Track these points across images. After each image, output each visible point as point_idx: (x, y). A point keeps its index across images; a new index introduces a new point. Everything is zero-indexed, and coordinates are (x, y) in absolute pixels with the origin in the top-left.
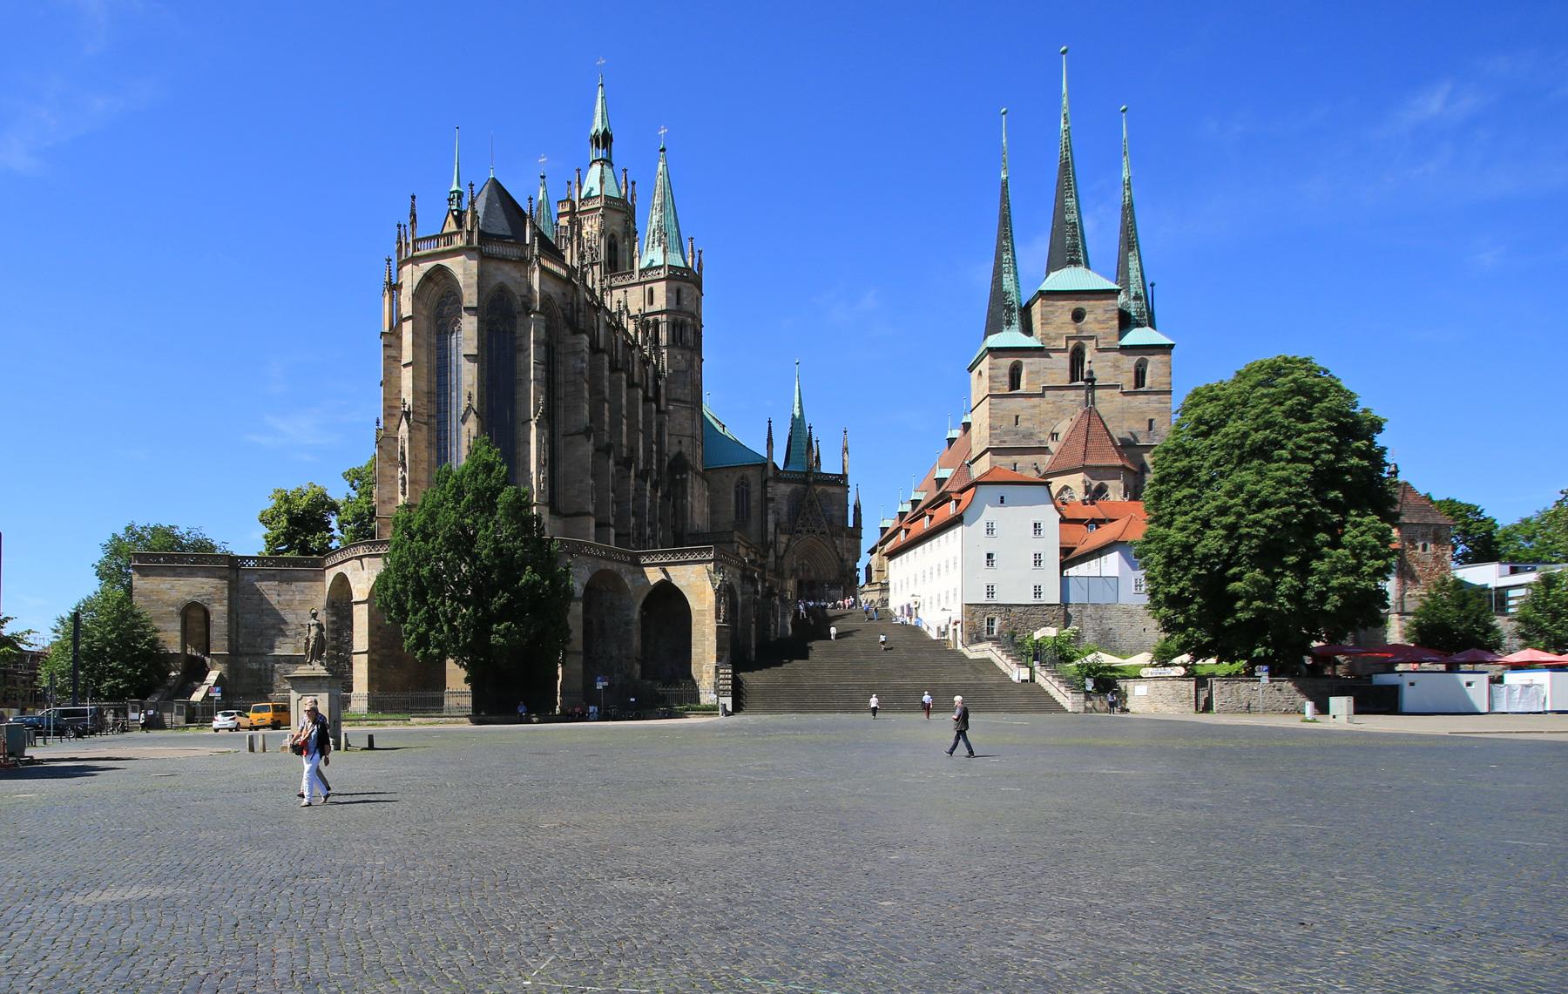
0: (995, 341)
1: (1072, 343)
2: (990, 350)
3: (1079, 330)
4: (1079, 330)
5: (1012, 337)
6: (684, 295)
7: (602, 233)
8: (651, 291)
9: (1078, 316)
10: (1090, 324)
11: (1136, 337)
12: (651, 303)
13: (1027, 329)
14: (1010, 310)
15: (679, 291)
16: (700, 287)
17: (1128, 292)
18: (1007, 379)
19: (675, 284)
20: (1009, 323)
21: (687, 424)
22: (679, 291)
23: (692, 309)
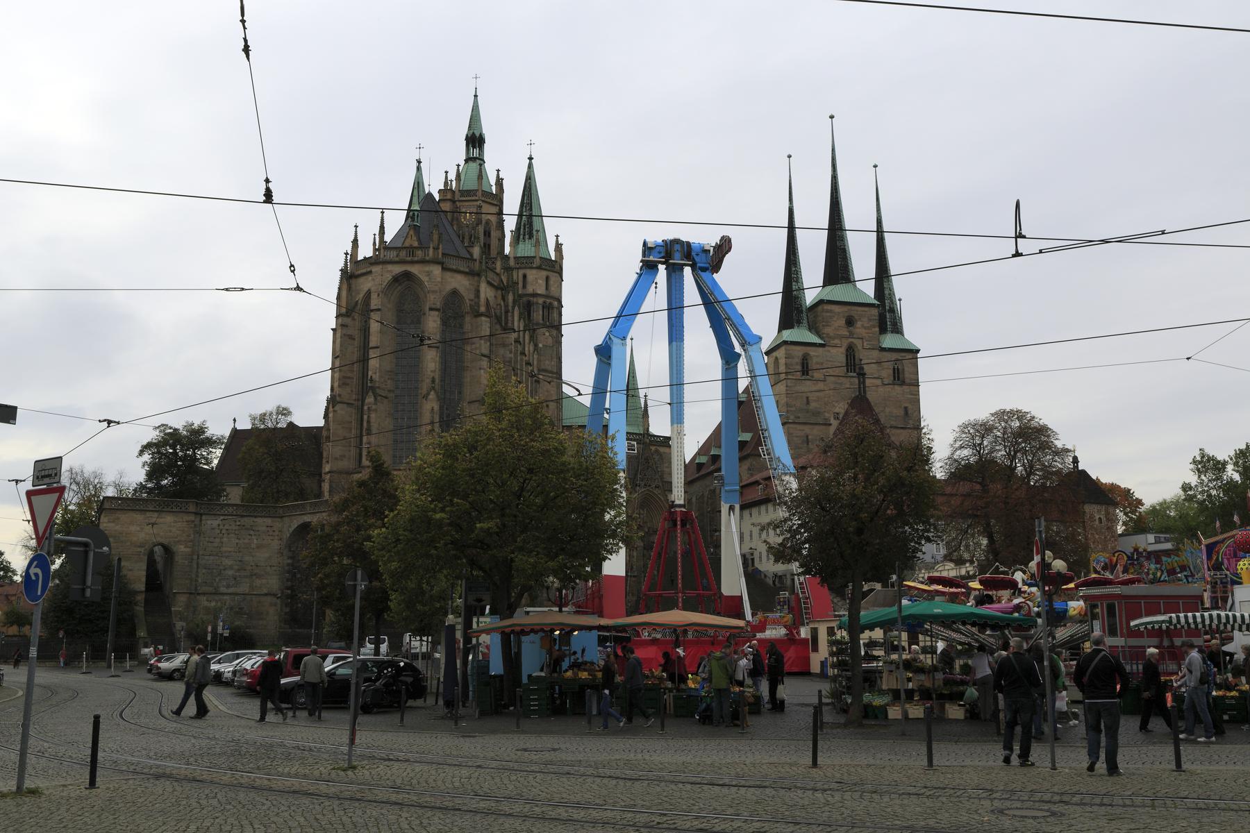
0: (788, 335)
1: (845, 343)
2: (785, 343)
3: (851, 333)
4: (851, 335)
5: (800, 334)
6: (551, 282)
7: (479, 222)
8: (525, 276)
9: (850, 322)
10: (859, 329)
11: (889, 341)
12: (524, 287)
13: (813, 328)
14: (800, 311)
15: (547, 278)
16: (560, 273)
17: (883, 305)
18: (799, 367)
19: (544, 273)
20: (799, 323)
21: (553, 391)
22: (547, 278)
23: (556, 295)
